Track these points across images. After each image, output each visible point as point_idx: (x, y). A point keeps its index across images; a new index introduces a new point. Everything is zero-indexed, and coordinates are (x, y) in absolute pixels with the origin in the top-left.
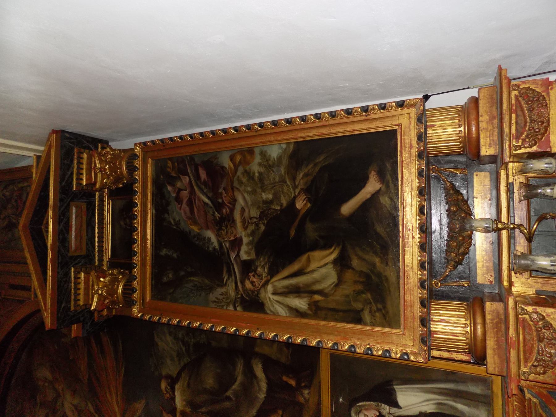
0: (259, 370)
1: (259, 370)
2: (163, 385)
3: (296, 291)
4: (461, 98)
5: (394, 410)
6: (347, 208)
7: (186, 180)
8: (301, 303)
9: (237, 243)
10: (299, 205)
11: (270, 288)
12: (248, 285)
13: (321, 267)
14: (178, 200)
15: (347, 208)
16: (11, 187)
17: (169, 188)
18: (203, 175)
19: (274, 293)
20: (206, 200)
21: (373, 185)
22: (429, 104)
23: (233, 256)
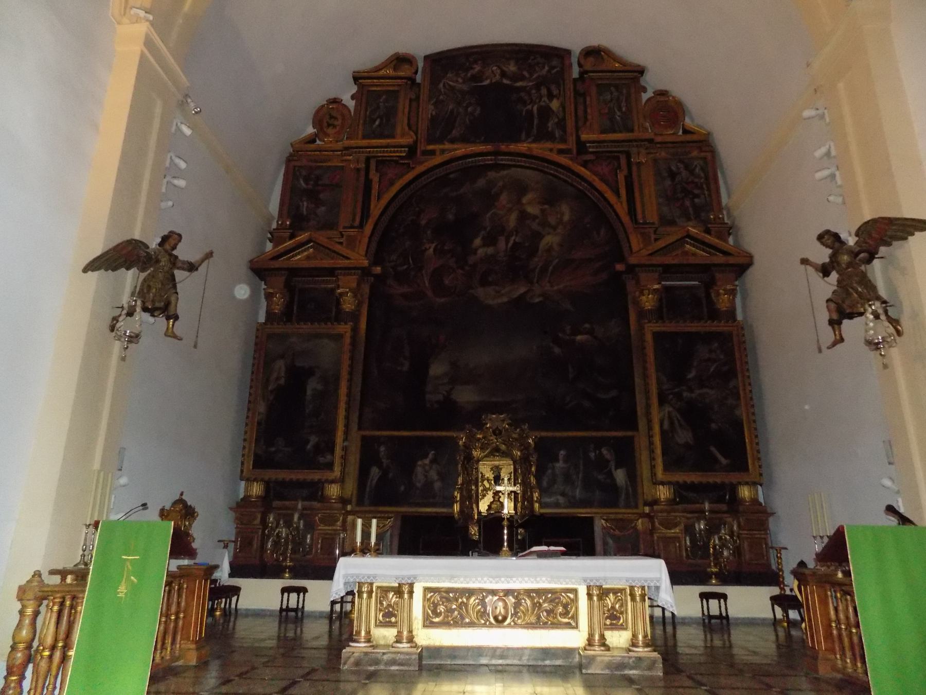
0: (614, 393)
1: (614, 393)
2: (587, 326)
3: (672, 423)
4: (761, 500)
5: (613, 467)
6: (713, 449)
7: (722, 357)
8: (666, 425)
9: (691, 390)
10: (713, 426)
11: (671, 409)
12: (671, 396)
13: (684, 436)
14: (711, 351)
15: (713, 449)
16: (702, 175)
17: (716, 345)
18: (725, 368)
19: (669, 413)
20: (712, 370)
21: (724, 461)
22: (759, 487)
23: (684, 388)
